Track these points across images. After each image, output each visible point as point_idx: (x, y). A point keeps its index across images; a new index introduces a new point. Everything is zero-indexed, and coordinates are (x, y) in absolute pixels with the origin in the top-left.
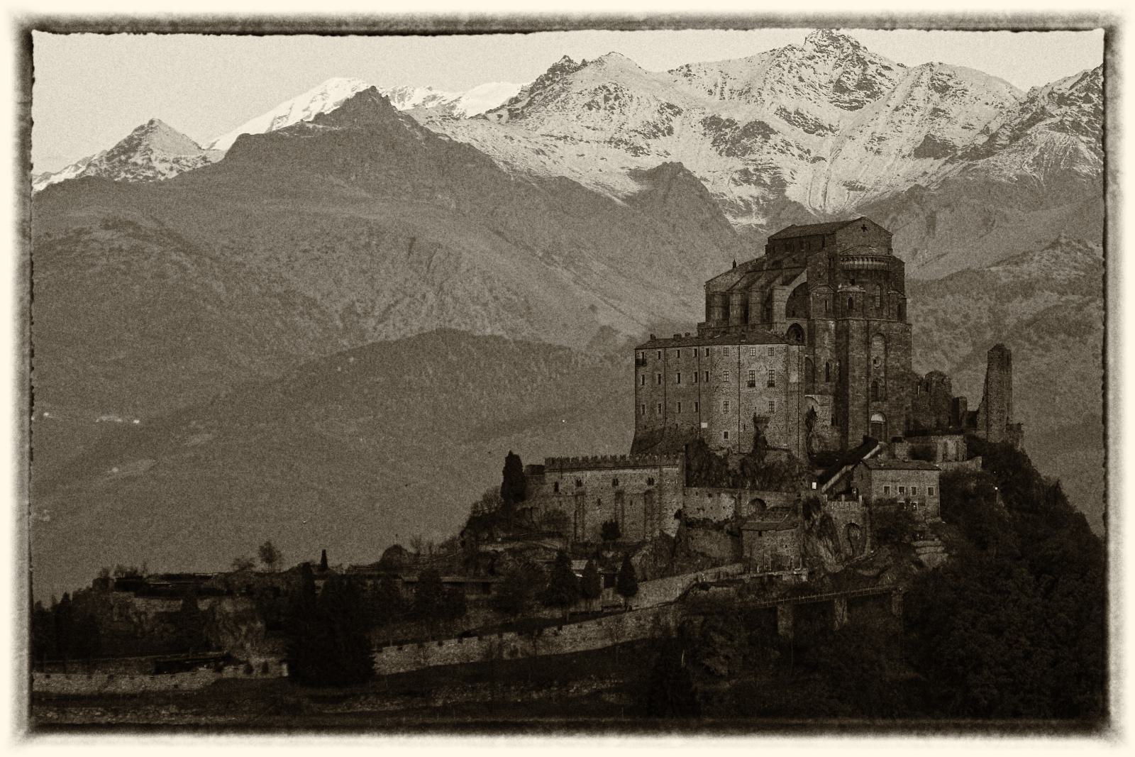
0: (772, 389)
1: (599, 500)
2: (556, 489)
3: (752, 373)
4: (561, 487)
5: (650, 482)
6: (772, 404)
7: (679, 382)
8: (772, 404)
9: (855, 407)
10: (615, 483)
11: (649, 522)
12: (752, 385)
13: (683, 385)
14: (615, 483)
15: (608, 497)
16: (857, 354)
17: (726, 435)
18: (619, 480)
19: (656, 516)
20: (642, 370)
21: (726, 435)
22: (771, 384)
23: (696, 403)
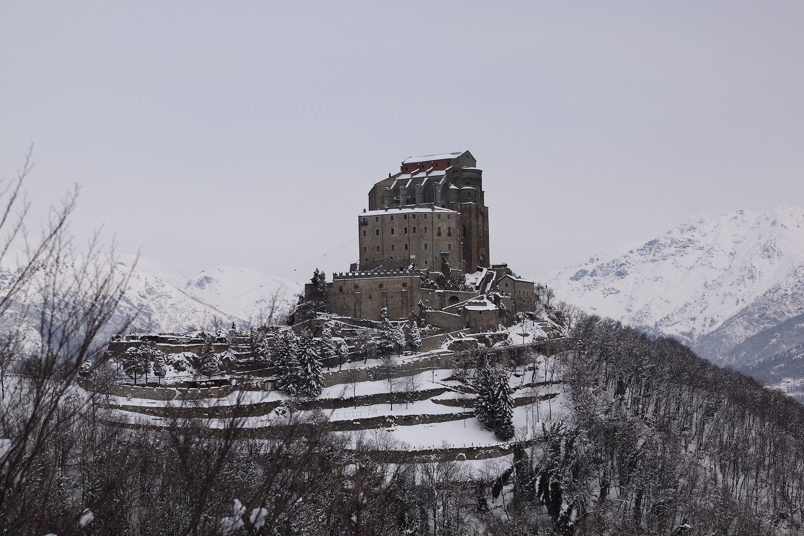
0: (450, 237)
1: (370, 296)
2: (341, 290)
3: (439, 228)
4: (344, 289)
5: (404, 285)
6: (450, 245)
7: (393, 233)
8: (450, 245)
9: (474, 252)
10: (381, 286)
11: (405, 308)
12: (439, 234)
13: (395, 235)
14: (381, 286)
15: (376, 295)
16: (474, 222)
17: (426, 263)
18: (384, 284)
19: (409, 304)
20: (364, 228)
21: (426, 263)
22: (449, 235)
23: (406, 245)
